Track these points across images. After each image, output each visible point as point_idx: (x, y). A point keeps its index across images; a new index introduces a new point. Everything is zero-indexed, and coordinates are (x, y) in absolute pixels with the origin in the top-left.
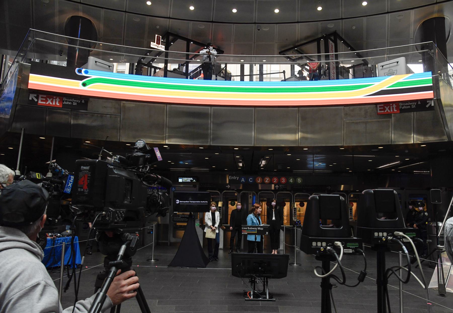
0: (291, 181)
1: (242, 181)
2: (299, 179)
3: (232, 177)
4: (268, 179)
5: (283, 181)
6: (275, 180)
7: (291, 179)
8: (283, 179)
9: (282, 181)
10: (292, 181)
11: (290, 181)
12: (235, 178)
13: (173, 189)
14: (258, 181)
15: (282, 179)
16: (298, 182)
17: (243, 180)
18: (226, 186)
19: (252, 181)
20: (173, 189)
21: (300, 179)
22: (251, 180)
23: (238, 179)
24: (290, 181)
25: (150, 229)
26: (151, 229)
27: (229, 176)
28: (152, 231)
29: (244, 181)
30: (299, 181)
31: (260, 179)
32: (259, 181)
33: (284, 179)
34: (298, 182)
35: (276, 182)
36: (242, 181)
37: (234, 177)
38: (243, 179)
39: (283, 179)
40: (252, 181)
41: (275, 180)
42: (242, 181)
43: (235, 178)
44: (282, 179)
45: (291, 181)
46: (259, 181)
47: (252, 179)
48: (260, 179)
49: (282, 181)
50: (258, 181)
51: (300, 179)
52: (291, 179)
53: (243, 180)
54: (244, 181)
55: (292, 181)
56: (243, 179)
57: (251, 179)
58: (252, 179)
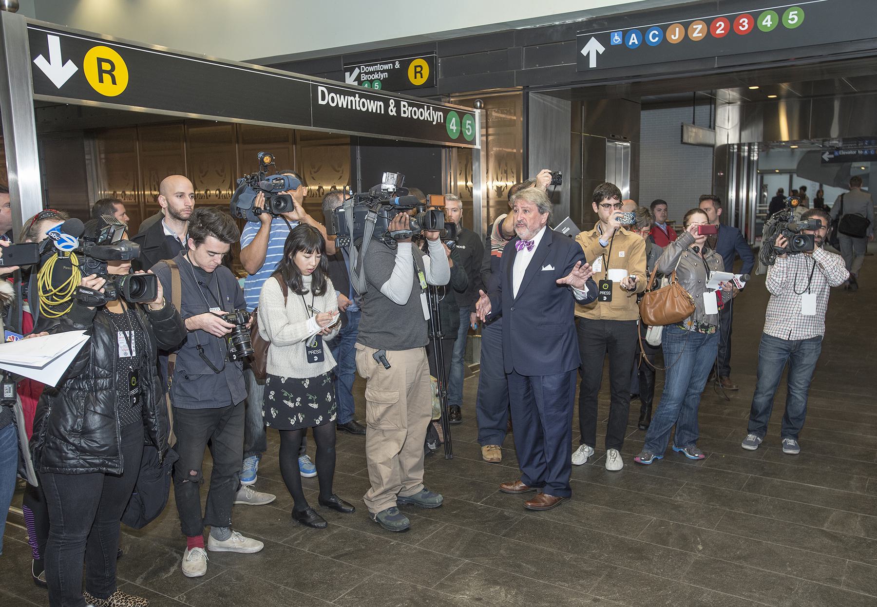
0: (767, 21)
2: (791, 13)
5: (744, 26)
6: (720, 25)
7: (769, 17)
8: (744, 22)
9: (740, 27)
10: (769, 24)
11: (764, 23)
14: (673, 36)
15: (741, 21)
16: (790, 22)
17: (634, 39)
18: (593, 64)
19: (657, 39)
21: (796, 12)
22: (654, 36)
24: (764, 23)
29: (637, 43)
30: (793, 19)
31: (677, 29)
33: (746, 20)
34: (790, 22)
35: (723, 32)
36: (630, 44)
38: (634, 35)
39: (744, 22)
40: (657, 39)
41: (720, 25)
42: (630, 44)
44: (741, 21)
45: (767, 21)
46: (675, 37)
47: (657, 33)
48: (677, 29)
49: (740, 27)
50: (673, 36)
51: (796, 12)
52: (769, 17)
53: (634, 39)
54: (637, 43)
55: (769, 24)
56: (634, 35)
58: (657, 33)
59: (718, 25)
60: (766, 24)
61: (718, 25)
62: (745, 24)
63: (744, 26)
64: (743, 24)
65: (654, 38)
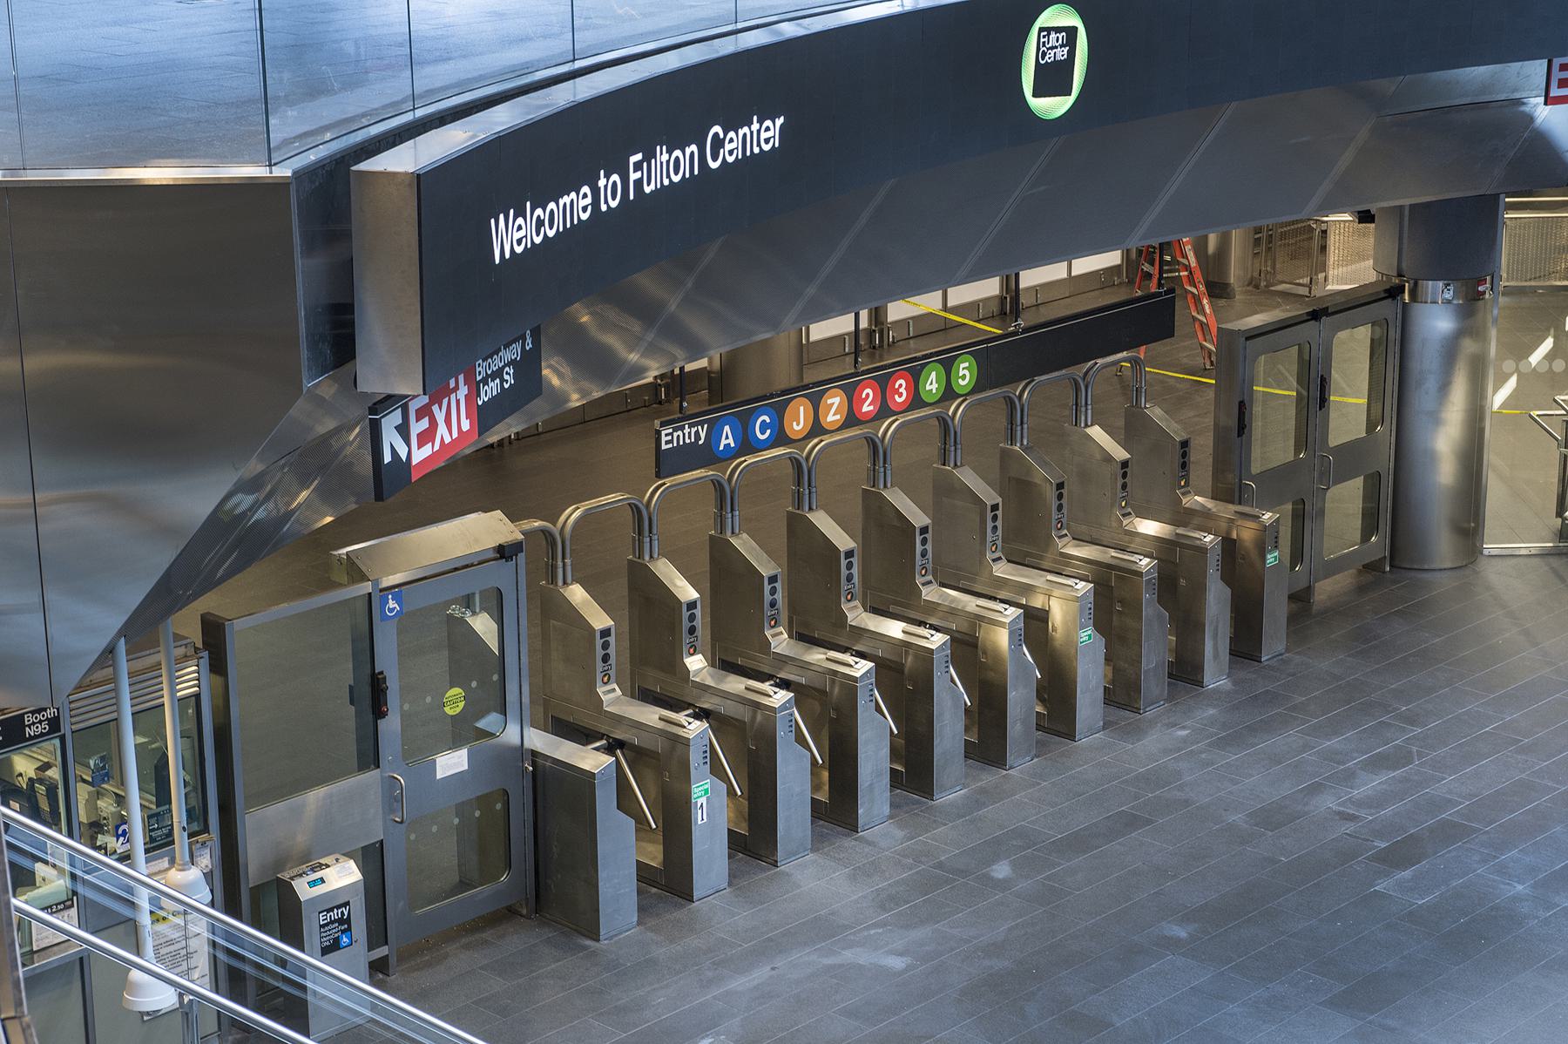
0: (931, 384)
1: (724, 442)
2: (962, 366)
3: (675, 435)
4: (836, 400)
5: (900, 395)
6: (868, 395)
12: (690, 433)
13: (392, 604)
14: (795, 423)
17: (727, 438)
20: (392, 604)
23: (703, 435)
24: (928, 387)
25: (335, 921)
26: (341, 921)
27: (663, 433)
28: (343, 932)
29: (733, 445)
32: (798, 425)
34: (960, 380)
36: (721, 448)
37: (687, 430)
38: (727, 428)
39: (901, 386)
41: (868, 395)
43: (690, 438)
45: (931, 384)
46: (798, 425)
53: (727, 438)
54: (733, 445)
56: (727, 428)
57: (764, 421)
59: (864, 396)
60: (931, 387)
61: (864, 396)
62: (902, 390)
63: (900, 395)
64: (900, 390)
65: (763, 433)
